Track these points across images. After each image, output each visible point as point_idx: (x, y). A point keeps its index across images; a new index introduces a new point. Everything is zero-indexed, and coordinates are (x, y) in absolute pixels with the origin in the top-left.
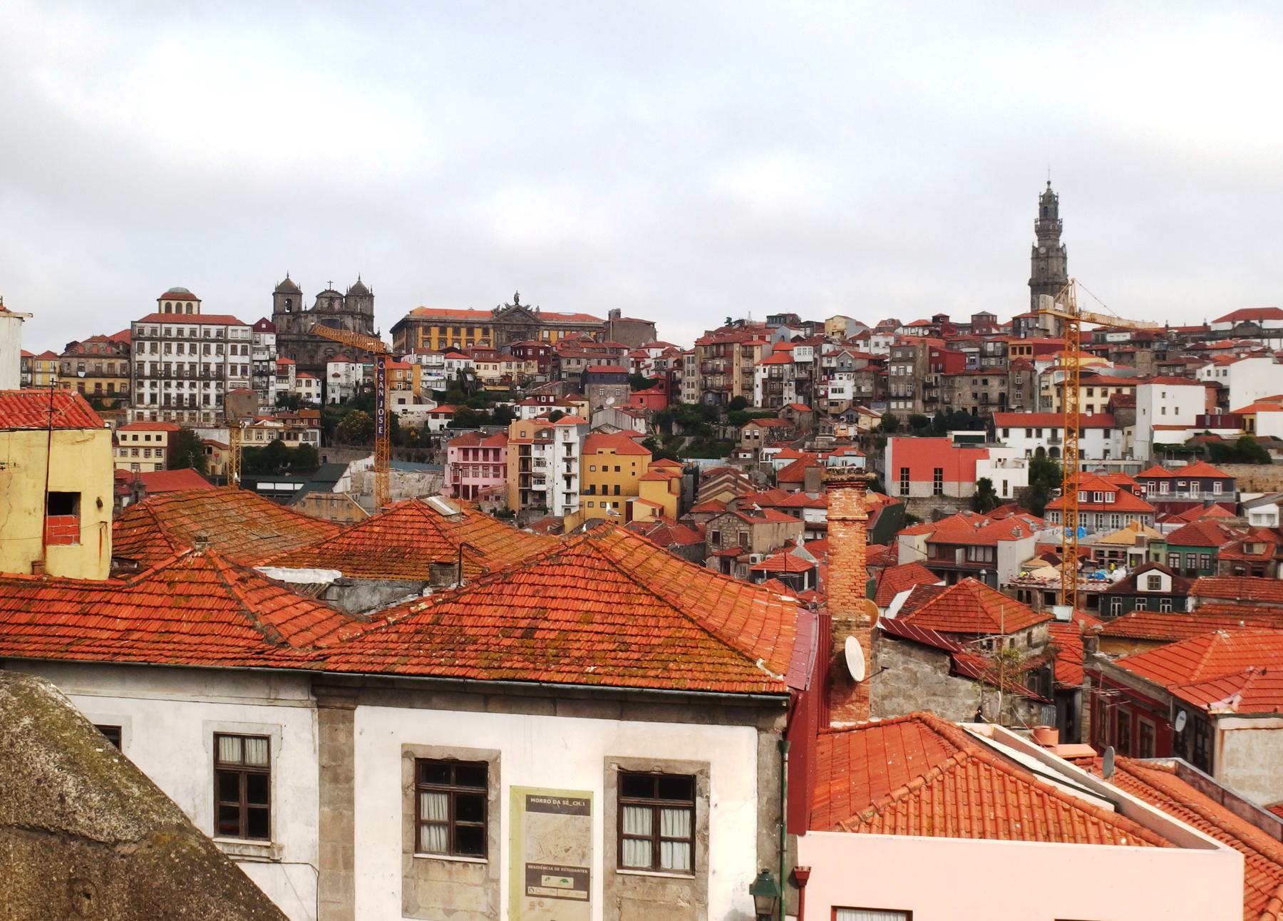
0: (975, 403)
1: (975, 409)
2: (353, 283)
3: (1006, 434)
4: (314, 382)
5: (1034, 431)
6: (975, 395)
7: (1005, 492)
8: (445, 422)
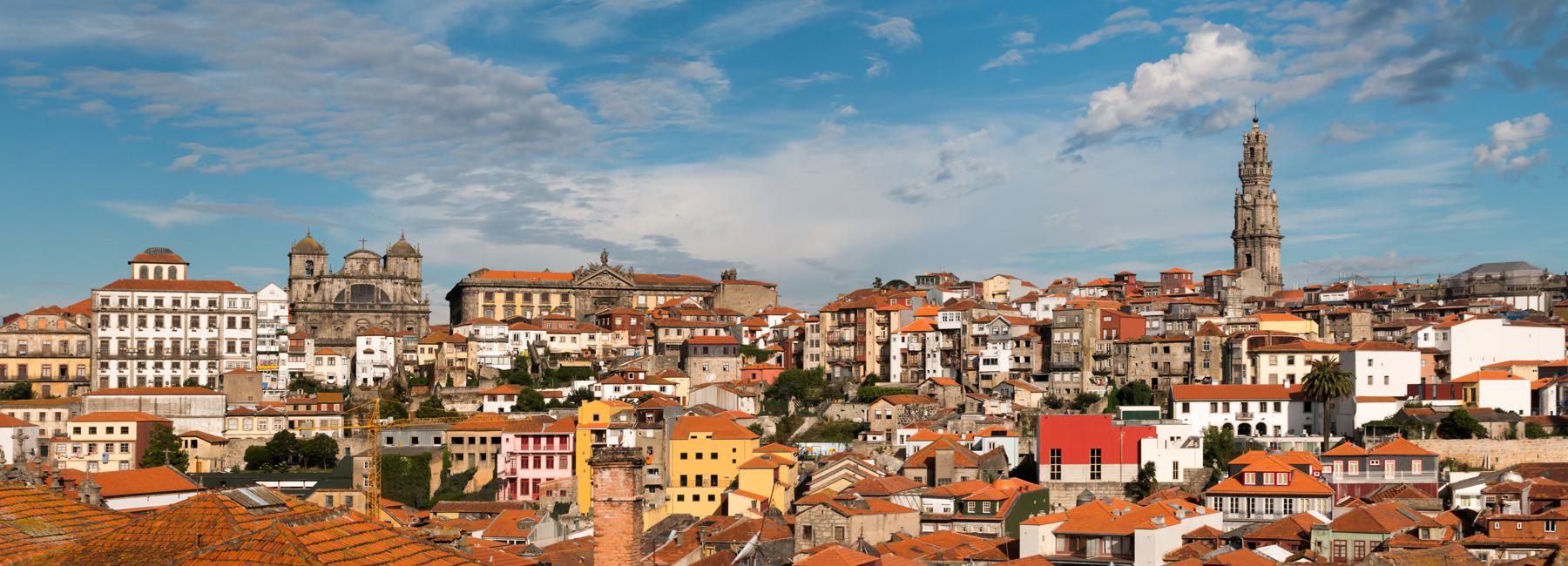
0: (1155, 374)
1: (1155, 381)
2: (394, 241)
3: (1186, 409)
4: (338, 358)
5: (1220, 405)
6: (1155, 365)
7: (1176, 476)
8: (507, 406)
